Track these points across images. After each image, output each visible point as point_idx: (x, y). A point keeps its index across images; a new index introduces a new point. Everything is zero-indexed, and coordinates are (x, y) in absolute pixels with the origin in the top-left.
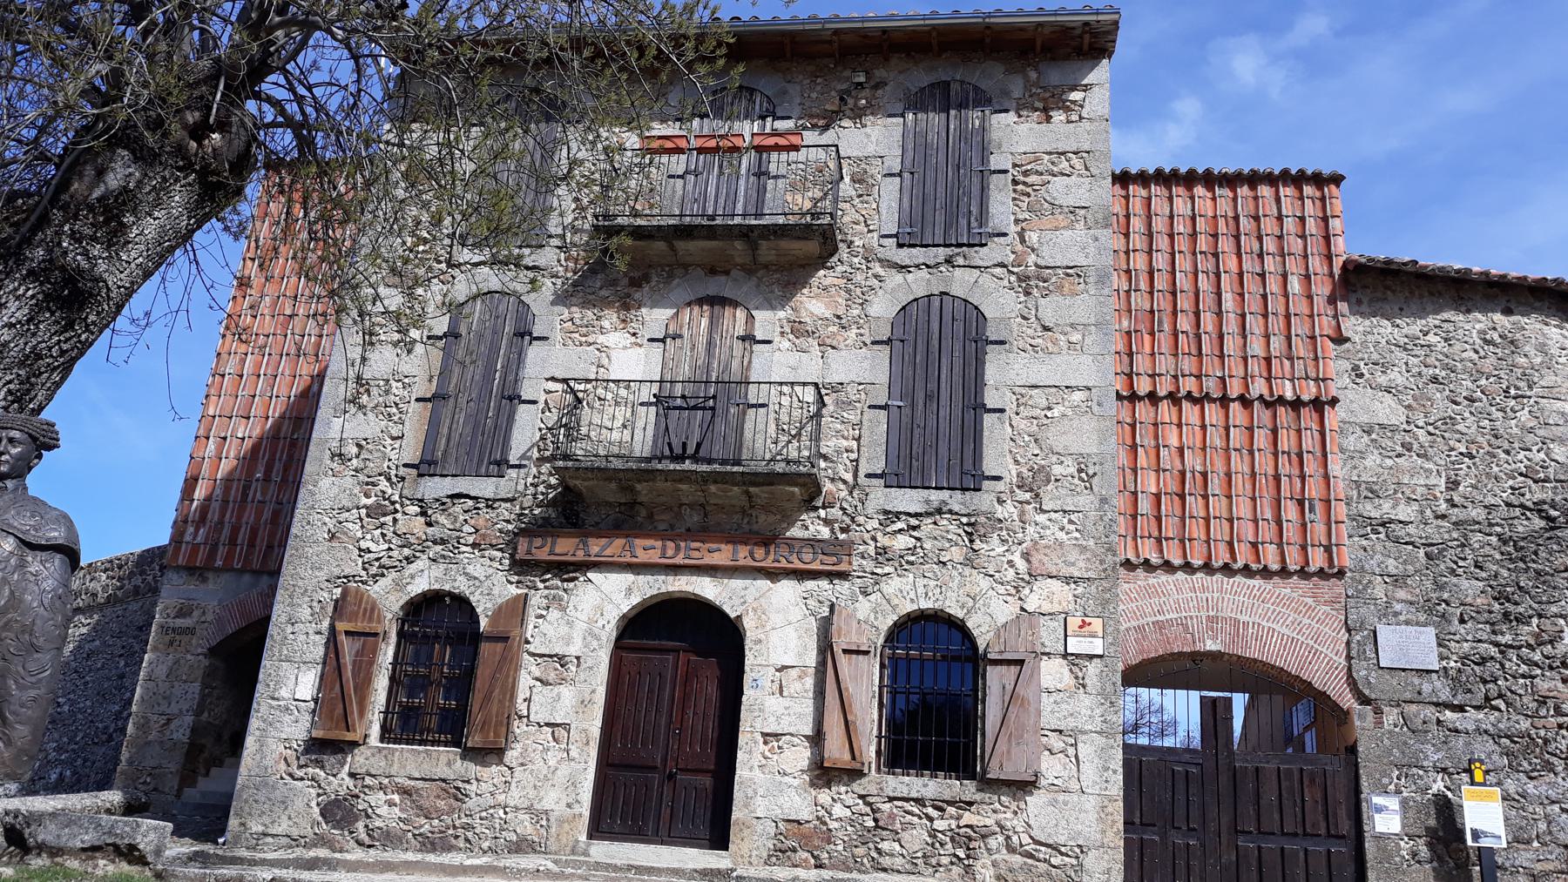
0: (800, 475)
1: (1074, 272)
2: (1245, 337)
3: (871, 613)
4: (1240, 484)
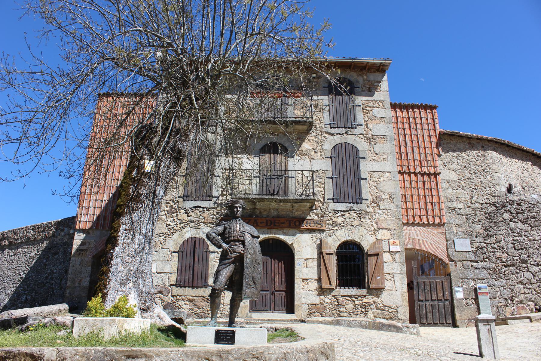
0: (311, 199)
1: (383, 137)
2: (413, 154)
3: (333, 243)
4: (415, 198)
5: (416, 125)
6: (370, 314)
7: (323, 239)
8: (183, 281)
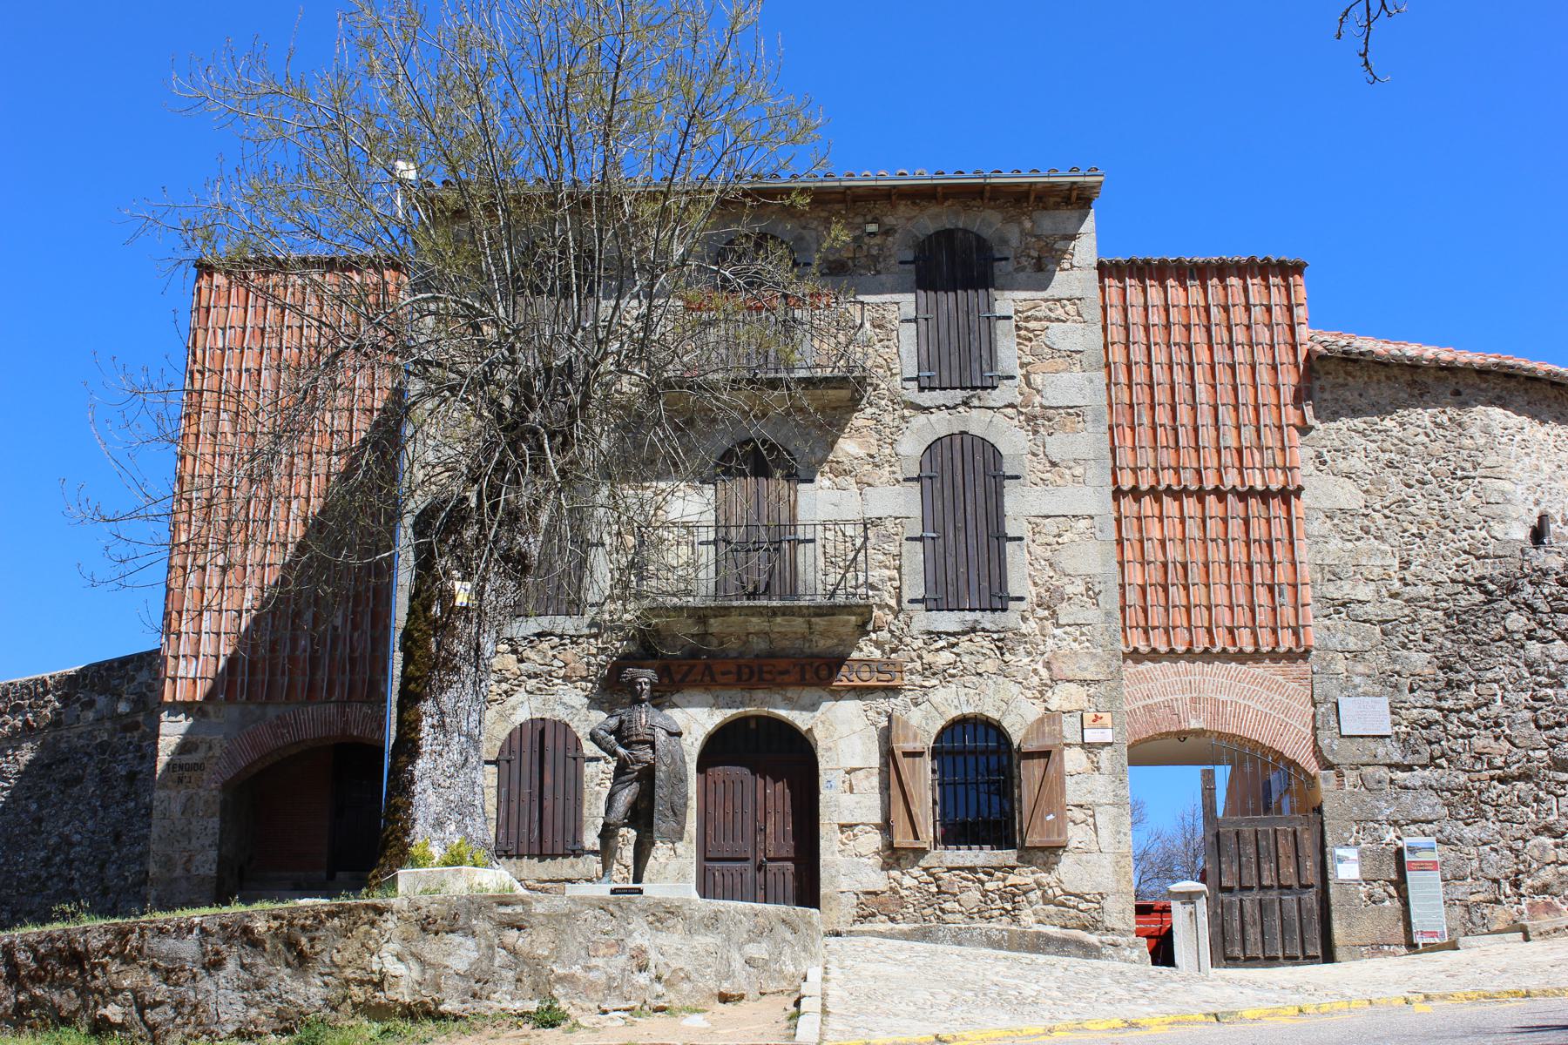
0: (858, 606)
1: (1074, 411)
2: (1217, 430)
3: (923, 722)
5: (1230, 330)
6: (1028, 918)
7: (896, 714)
8: (514, 841)
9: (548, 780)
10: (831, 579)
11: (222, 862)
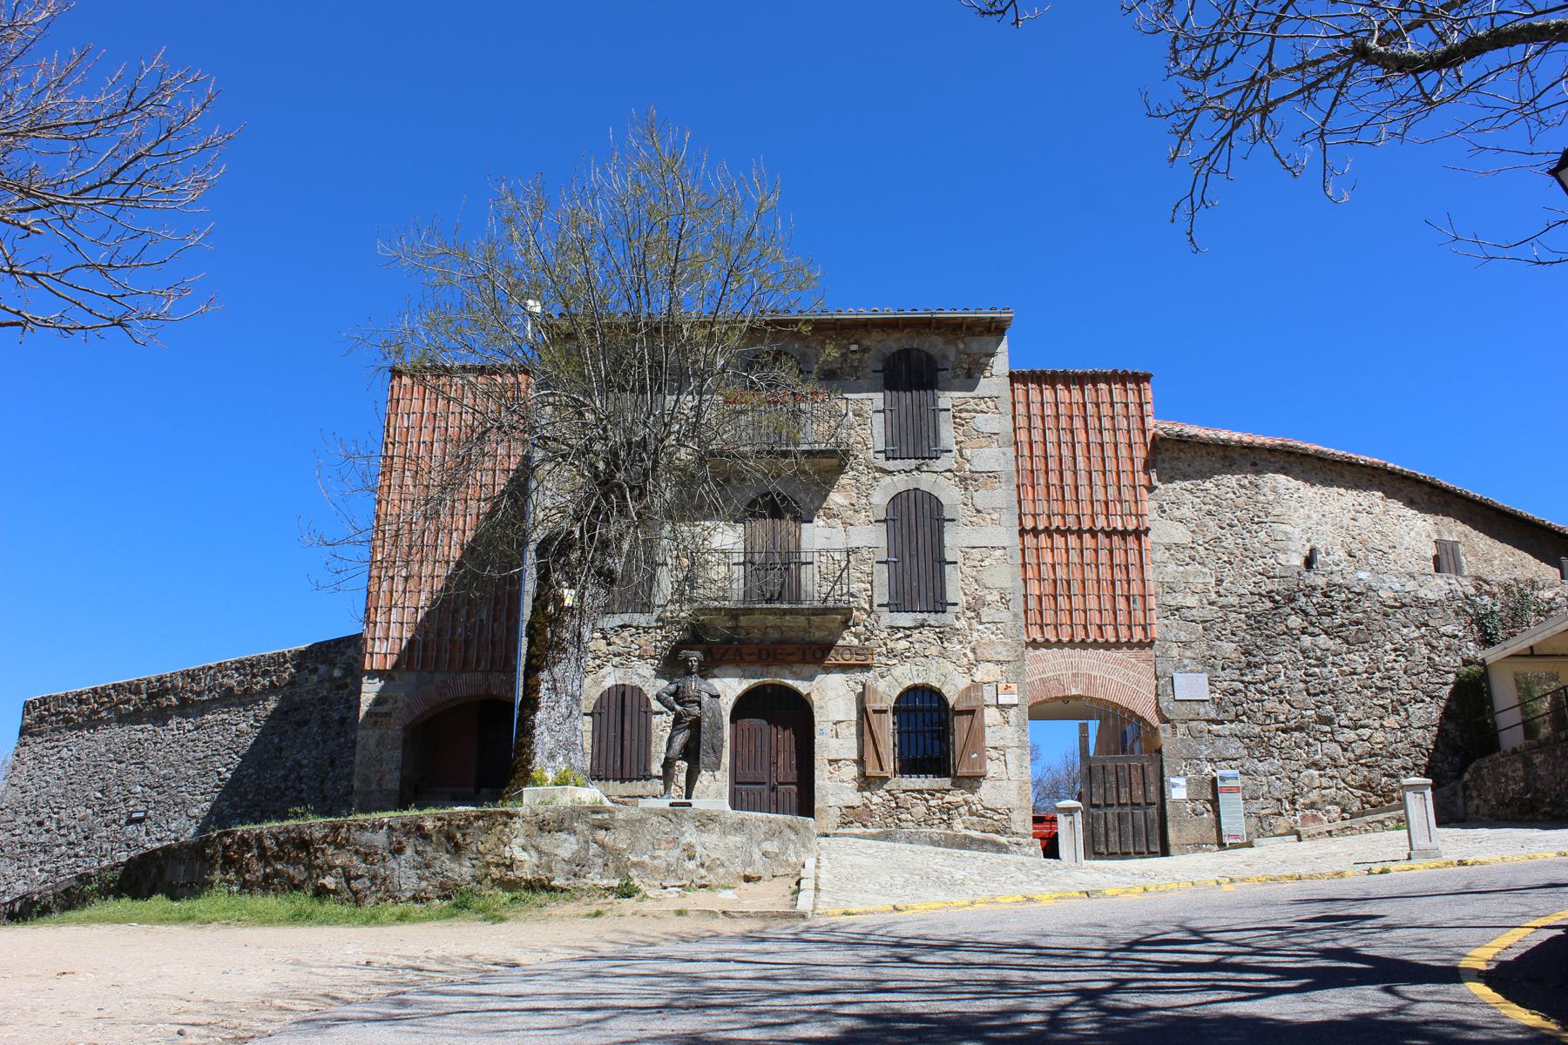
1: (993, 475)
3: (888, 687)
4: (1091, 587)
6: (958, 826)
9: (627, 727)
10: (825, 590)
11: (403, 781)
